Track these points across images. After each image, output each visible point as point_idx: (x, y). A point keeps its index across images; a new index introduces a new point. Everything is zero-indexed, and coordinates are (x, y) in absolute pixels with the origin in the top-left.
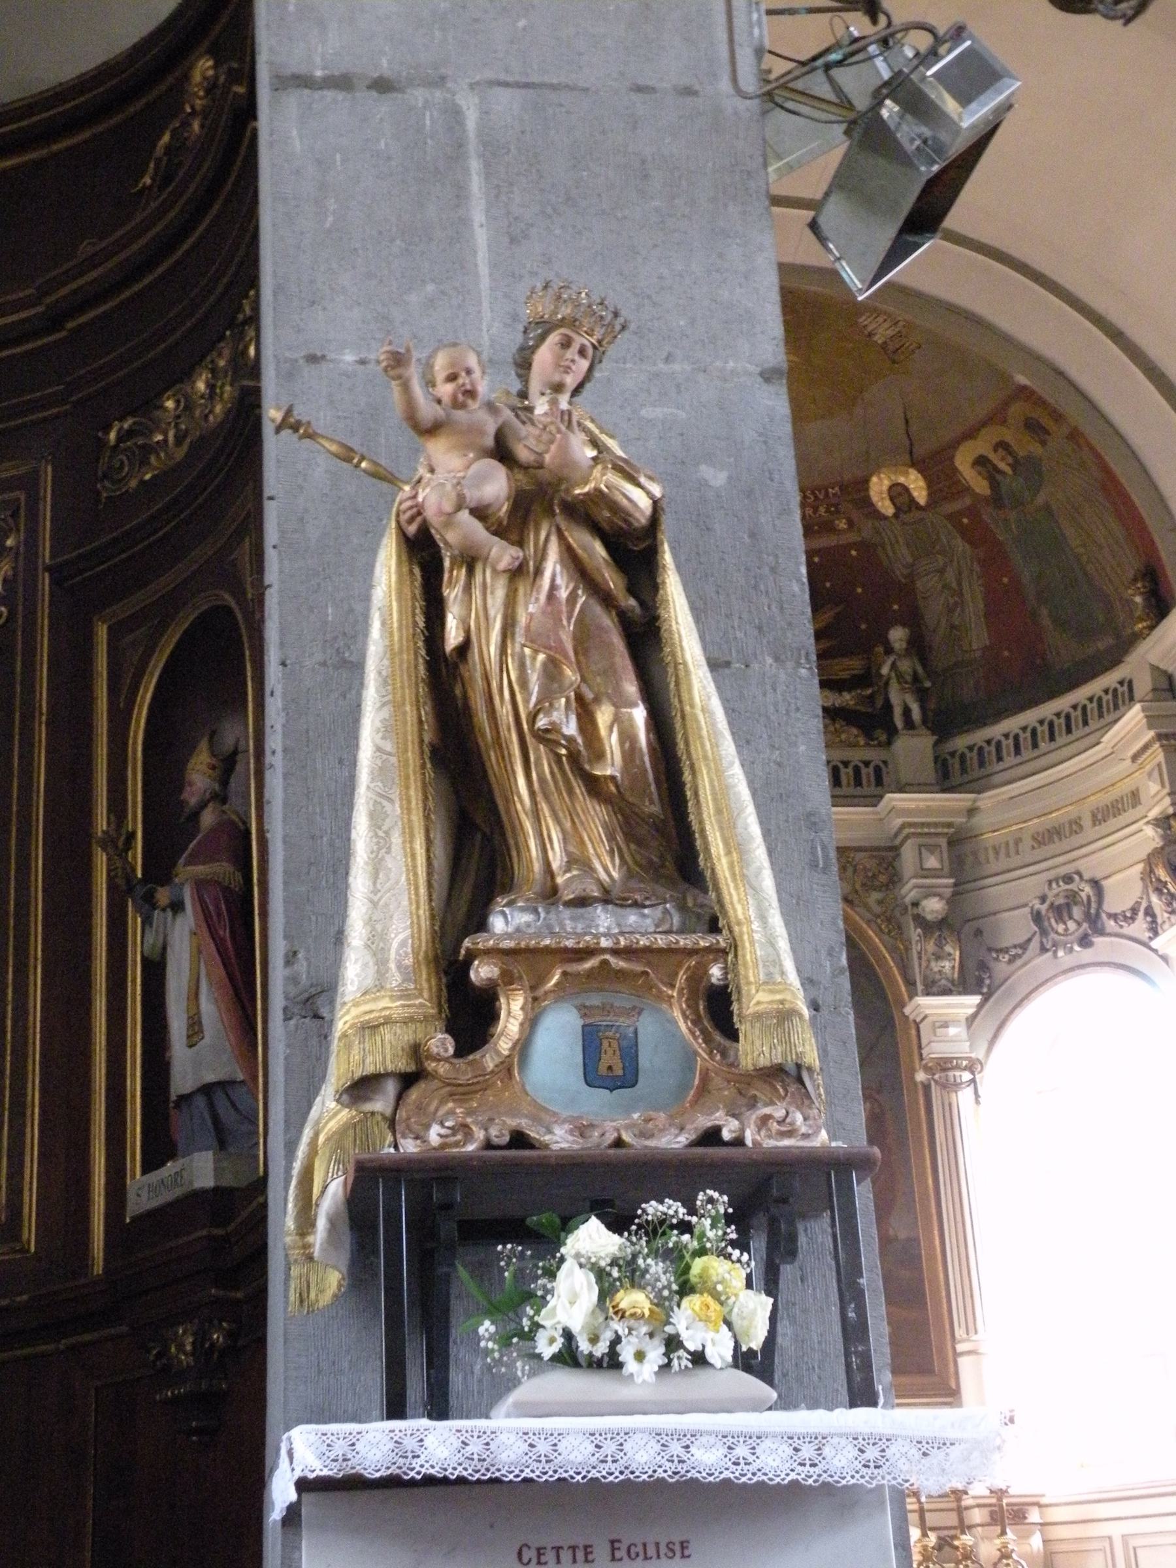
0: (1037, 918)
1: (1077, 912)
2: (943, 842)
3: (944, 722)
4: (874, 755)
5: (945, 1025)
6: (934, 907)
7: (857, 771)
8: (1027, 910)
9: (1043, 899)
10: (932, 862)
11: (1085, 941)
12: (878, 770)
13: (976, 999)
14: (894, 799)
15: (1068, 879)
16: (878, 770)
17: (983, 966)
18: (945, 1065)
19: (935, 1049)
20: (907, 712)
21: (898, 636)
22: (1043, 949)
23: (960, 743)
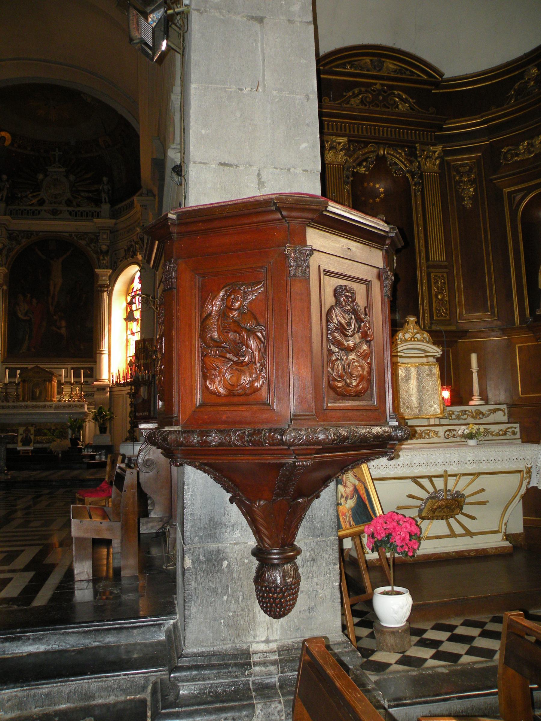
0: (125, 251)
1: (131, 249)
2: (108, 232)
3: (113, 202)
4: (97, 209)
5: (103, 276)
6: (104, 247)
7: (93, 213)
8: (123, 250)
9: (127, 246)
10: (105, 236)
11: (132, 257)
12: (98, 213)
13: (111, 271)
14: (95, 220)
15: (131, 242)
16: (98, 213)
17: (115, 263)
18: (103, 286)
19: (100, 282)
20: (105, 199)
21: (105, 179)
22: (126, 259)
23: (117, 207)
